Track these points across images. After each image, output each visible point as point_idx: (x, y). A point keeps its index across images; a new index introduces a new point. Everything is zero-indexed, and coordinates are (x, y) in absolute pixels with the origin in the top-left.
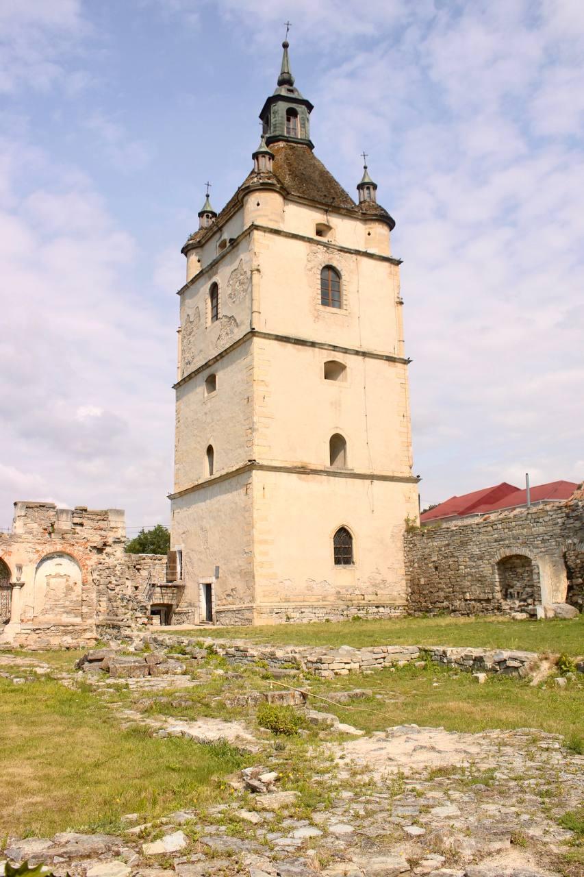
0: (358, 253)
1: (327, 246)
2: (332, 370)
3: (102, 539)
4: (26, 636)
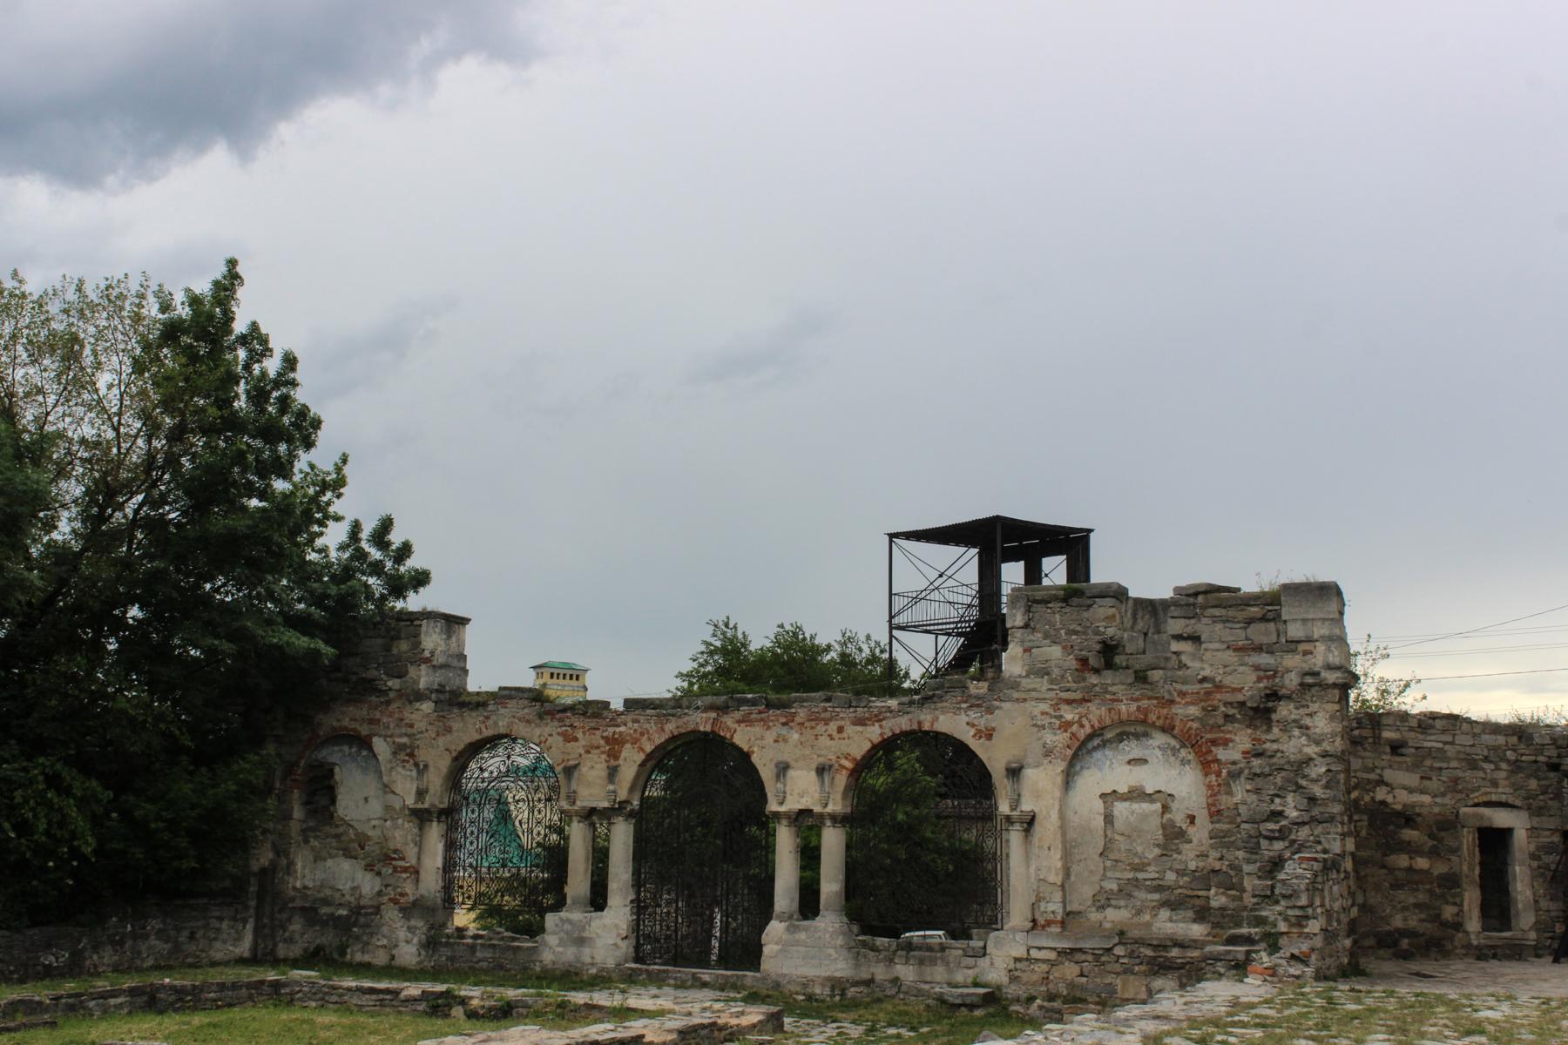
3: (1260, 679)
4: (1045, 967)
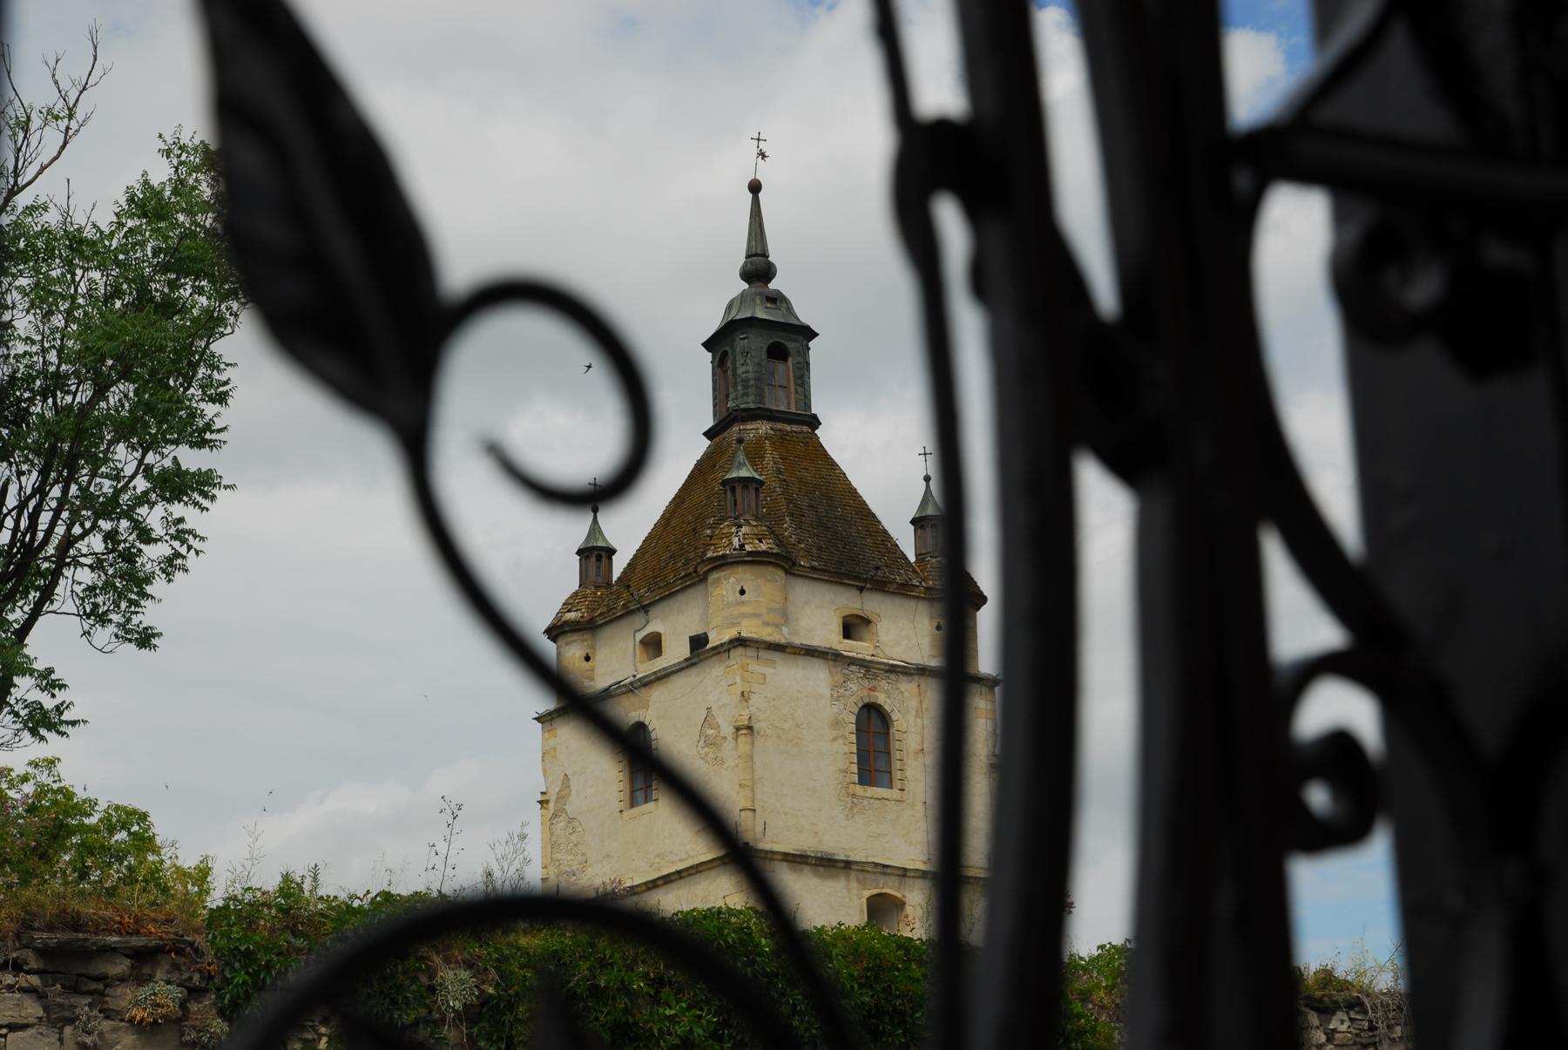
1: (866, 666)
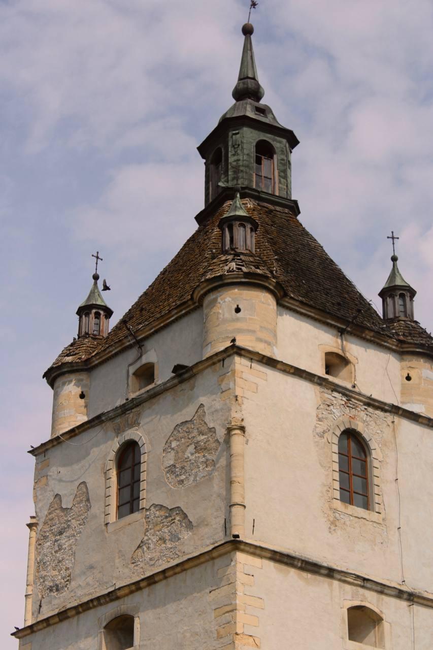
0: (395, 410)
1: (348, 394)
2: (361, 621)
